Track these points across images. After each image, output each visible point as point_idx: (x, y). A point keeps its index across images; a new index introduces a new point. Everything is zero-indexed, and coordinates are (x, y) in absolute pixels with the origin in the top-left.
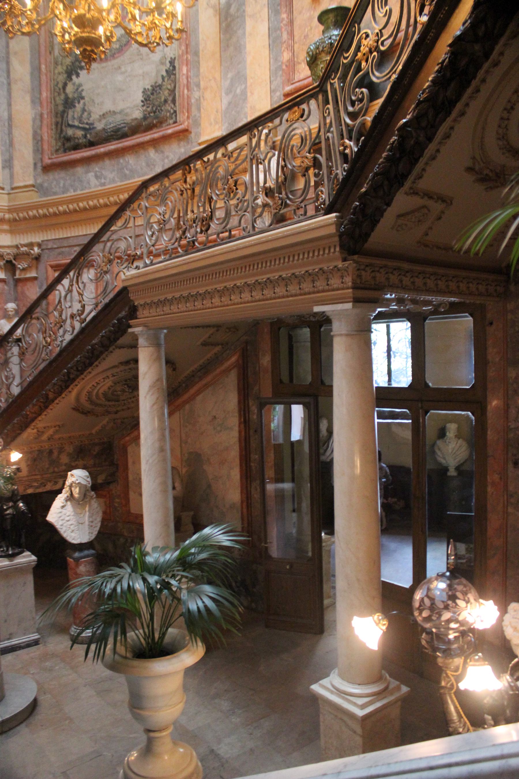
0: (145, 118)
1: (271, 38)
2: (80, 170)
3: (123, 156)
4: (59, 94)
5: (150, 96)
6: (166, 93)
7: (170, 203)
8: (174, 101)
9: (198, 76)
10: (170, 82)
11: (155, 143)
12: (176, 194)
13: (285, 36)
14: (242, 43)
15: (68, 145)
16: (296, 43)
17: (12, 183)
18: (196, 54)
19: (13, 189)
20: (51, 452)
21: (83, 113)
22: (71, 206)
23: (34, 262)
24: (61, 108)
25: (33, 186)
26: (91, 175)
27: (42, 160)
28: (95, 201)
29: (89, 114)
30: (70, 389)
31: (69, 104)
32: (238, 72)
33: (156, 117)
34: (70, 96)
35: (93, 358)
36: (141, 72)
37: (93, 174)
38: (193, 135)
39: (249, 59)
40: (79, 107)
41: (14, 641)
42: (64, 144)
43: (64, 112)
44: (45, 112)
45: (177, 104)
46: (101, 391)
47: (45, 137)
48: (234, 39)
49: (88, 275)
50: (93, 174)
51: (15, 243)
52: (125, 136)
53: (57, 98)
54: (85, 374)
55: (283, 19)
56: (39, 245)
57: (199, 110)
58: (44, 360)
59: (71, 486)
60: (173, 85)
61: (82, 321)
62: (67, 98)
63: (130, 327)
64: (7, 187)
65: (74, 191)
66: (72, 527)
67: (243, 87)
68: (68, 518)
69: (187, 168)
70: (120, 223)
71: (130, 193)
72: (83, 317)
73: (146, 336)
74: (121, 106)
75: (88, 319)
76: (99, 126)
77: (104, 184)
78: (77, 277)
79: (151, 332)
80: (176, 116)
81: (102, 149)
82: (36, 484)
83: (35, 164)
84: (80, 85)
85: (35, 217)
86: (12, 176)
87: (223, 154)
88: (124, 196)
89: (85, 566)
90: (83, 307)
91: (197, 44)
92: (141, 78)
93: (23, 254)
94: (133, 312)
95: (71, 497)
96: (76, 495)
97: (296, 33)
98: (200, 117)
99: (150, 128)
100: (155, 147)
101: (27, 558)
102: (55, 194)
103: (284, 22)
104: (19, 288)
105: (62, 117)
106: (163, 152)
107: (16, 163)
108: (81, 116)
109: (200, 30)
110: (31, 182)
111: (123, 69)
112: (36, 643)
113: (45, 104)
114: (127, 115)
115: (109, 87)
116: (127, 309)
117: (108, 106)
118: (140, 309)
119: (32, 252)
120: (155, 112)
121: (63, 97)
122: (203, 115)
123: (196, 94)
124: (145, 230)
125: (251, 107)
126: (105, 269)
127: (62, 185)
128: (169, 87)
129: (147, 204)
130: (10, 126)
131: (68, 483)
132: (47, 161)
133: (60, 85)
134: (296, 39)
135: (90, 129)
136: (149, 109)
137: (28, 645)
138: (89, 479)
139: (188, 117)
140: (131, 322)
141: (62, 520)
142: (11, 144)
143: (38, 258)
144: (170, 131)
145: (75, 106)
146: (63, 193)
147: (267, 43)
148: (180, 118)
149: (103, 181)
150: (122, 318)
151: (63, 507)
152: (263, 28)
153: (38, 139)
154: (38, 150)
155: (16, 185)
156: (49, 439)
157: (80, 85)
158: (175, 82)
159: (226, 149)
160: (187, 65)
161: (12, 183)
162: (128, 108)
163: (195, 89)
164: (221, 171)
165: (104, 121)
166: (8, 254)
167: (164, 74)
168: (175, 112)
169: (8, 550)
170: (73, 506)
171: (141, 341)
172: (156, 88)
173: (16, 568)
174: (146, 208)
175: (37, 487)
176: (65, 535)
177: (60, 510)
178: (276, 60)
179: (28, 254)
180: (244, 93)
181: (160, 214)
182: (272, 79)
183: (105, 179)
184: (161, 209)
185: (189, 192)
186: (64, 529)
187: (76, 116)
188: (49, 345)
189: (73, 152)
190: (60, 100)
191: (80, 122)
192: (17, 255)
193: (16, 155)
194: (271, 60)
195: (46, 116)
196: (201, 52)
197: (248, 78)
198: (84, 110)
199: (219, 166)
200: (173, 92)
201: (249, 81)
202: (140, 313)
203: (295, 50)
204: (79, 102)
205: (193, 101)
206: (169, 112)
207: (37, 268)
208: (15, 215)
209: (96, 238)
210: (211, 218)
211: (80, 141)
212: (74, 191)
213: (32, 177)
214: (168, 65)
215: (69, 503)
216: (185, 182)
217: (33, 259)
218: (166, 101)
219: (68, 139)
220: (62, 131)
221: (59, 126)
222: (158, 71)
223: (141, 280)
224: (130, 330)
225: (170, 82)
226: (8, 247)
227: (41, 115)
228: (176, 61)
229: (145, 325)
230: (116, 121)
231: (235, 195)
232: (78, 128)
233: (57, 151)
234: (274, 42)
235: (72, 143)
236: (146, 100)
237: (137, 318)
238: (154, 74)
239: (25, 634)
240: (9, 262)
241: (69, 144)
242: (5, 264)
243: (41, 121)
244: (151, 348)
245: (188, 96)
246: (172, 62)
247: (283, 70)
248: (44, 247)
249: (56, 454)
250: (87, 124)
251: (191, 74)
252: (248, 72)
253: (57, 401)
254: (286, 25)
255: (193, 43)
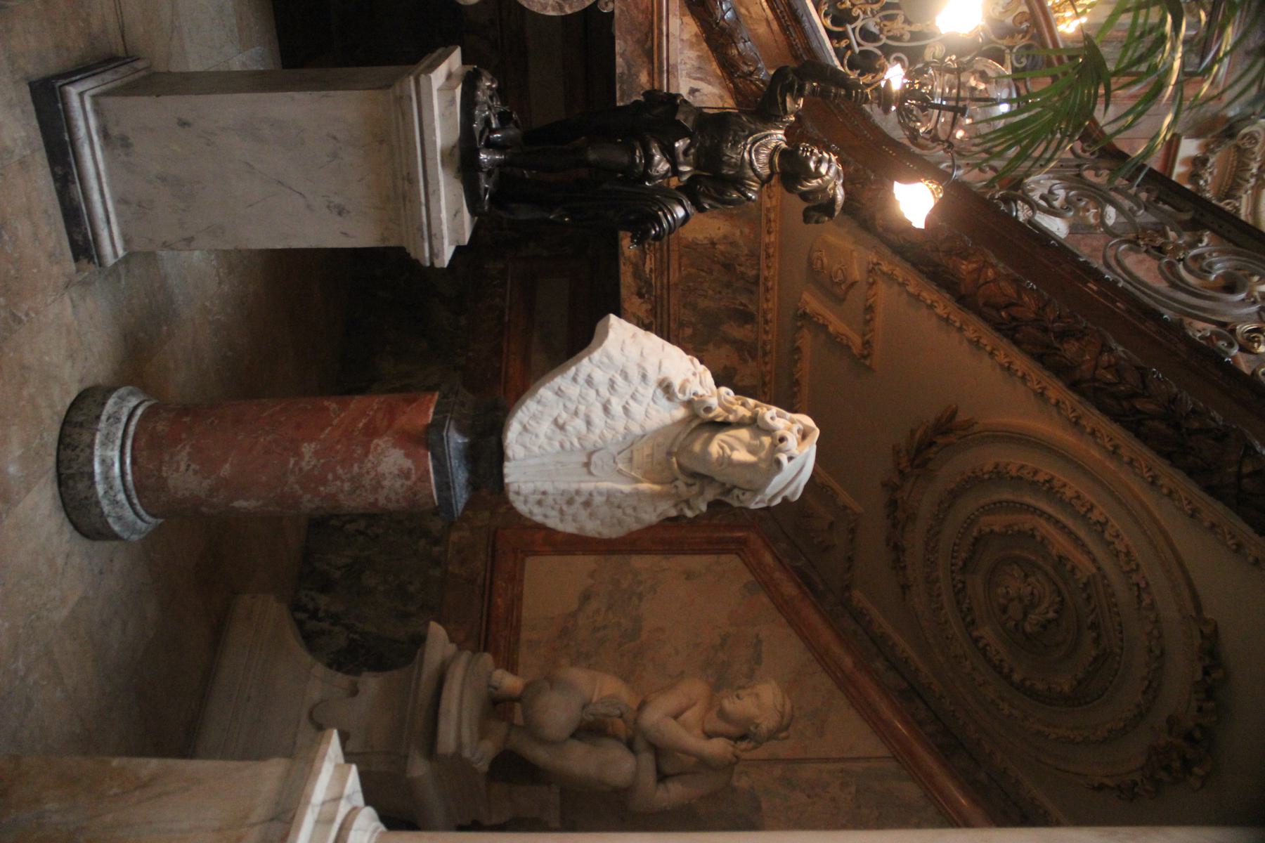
20: (745, 317)
41: (93, 158)
59: (754, 423)
66: (580, 424)
68: (616, 407)
82: (648, 266)
89: (405, 474)
95: (704, 423)
96: (717, 445)
101: (448, 223)
112: (84, 247)
131: (771, 414)
137: (74, 216)
141: (612, 384)
151: (666, 388)
169: (490, 145)
170: (662, 431)
173: (411, 181)
175: (638, 274)
176: (545, 393)
177: (653, 377)
186: (573, 391)
188: (1242, 349)
215: (680, 413)
239: (121, 201)
249: (737, 332)
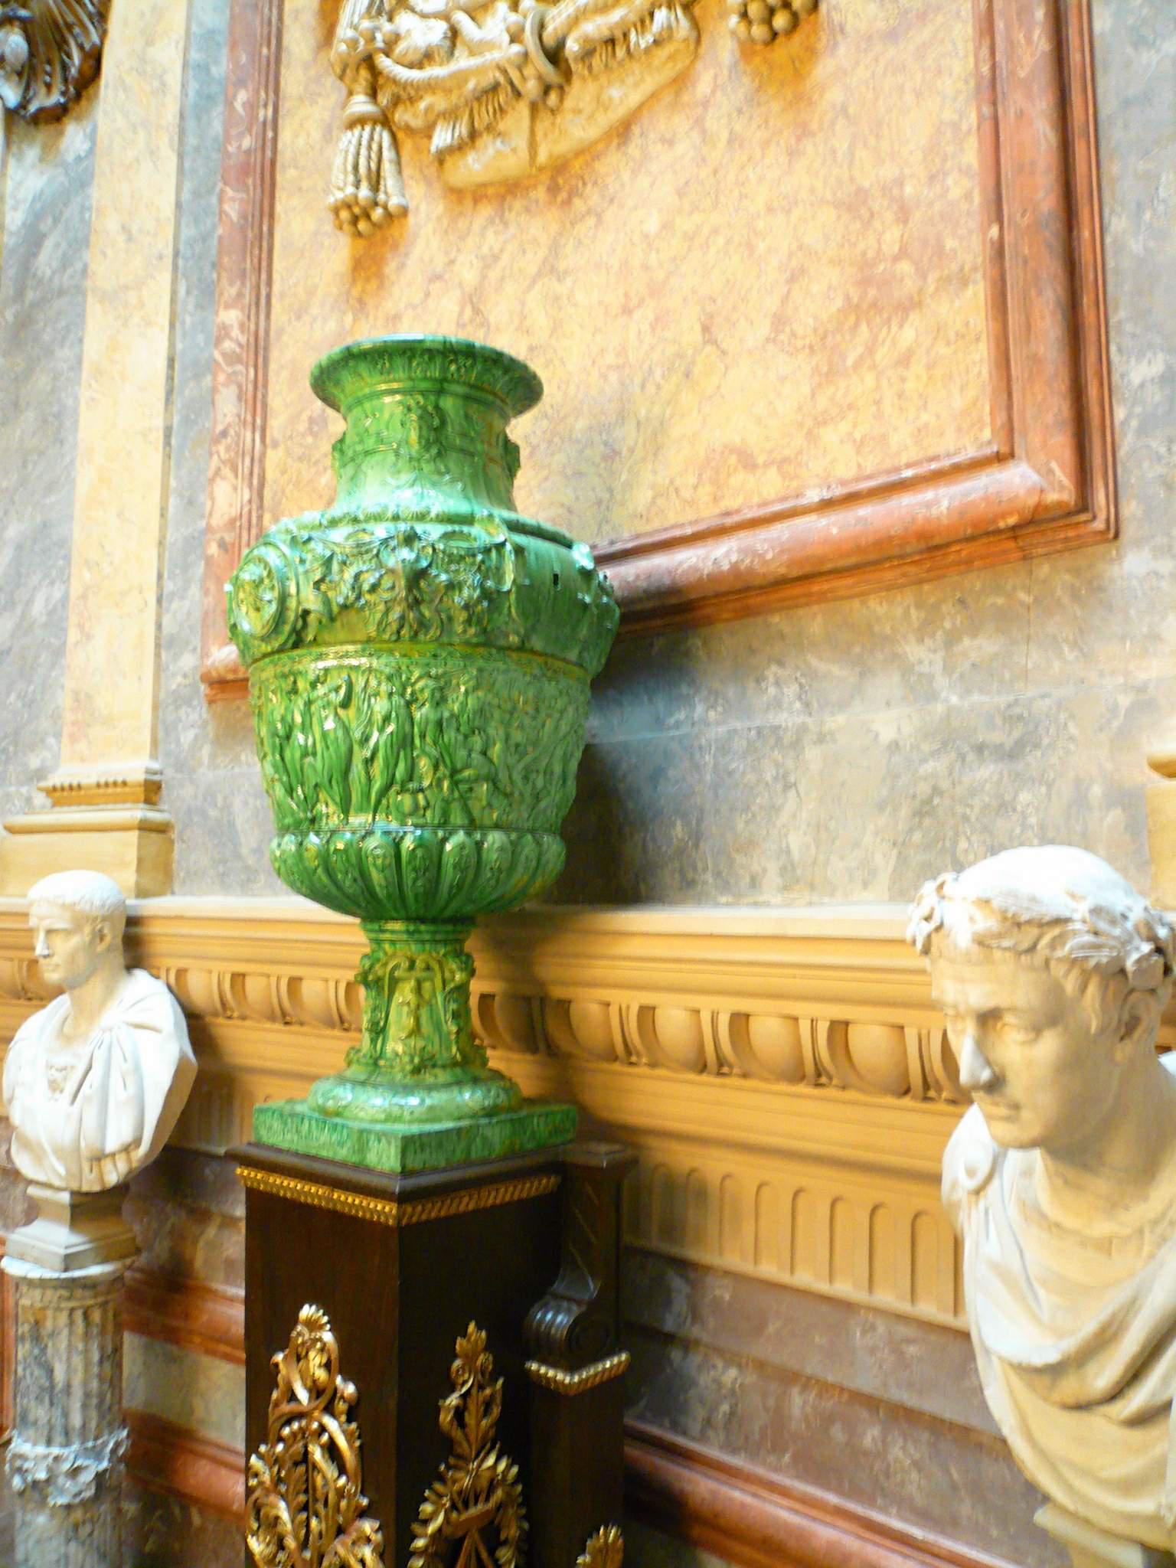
1: (178, 402)
13: (228, 407)
14: (70, 402)
16: (275, 445)
32: (45, 525)
39: (85, 478)
48: (42, 381)
55: (224, 332)
67: (57, 593)
97: (275, 402)
103: (228, 345)
125: (76, 694)
134: (276, 425)
147: (159, 423)
152: (146, 354)
178: (191, 502)
180: (56, 619)
182: (169, 586)
194: (172, 501)
197: (76, 559)
201: (80, 578)
203: (270, 475)
234: (187, 421)
247: (209, 561)
252: (77, 535)
254: (232, 358)
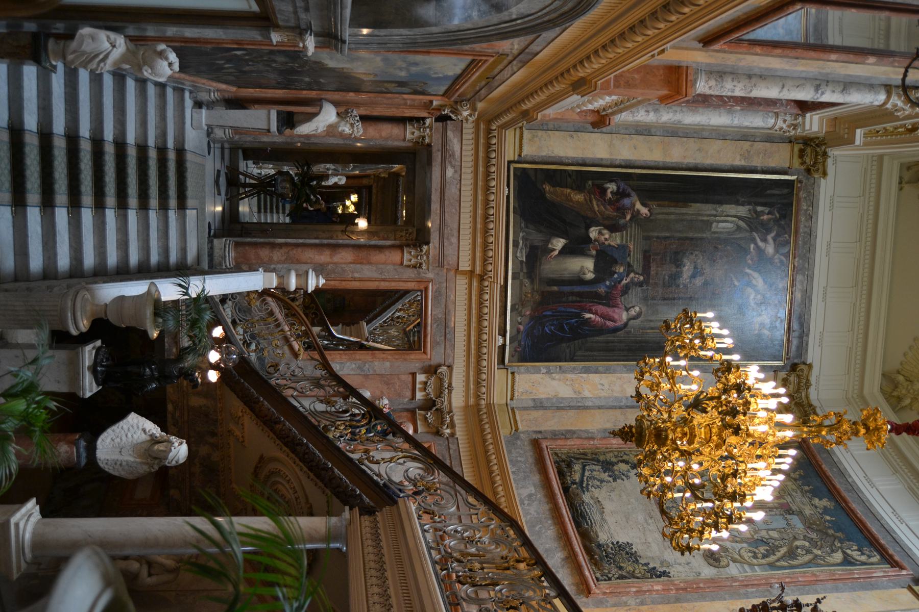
0: (599, 546)
2: (536, 478)
3: (555, 524)
4: (616, 456)
5: (624, 550)
6: (630, 568)
7: (493, 547)
8: (621, 577)
9: (654, 602)
10: (643, 572)
11: (571, 558)
12: (505, 553)
15: (563, 465)
17: (519, 409)
18: (677, 600)
19: (513, 409)
20: (214, 434)
21: (598, 480)
22: (496, 467)
23: (434, 430)
24: (602, 458)
25: (517, 430)
26: (532, 490)
27: (546, 438)
28: (502, 493)
29: (598, 487)
30: (285, 448)
31: (608, 466)
33: (601, 559)
34: (615, 467)
35: (316, 470)
36: (650, 540)
37: (533, 492)
38: (585, 599)
40: (605, 476)
42: (563, 461)
43: (598, 461)
44: (596, 442)
45: (619, 581)
46: (280, 487)
47: (569, 442)
49: (414, 469)
50: (533, 492)
51: (454, 410)
52: (578, 525)
53: (611, 454)
54: (301, 464)
56: (453, 435)
57: (614, 605)
58: (319, 422)
59: (169, 441)
60: (639, 575)
61: (361, 461)
62: (613, 464)
63: (351, 509)
64: (514, 404)
65: (513, 472)
66: (118, 440)
68: (129, 435)
69: (533, 562)
70: (471, 500)
71: (506, 510)
72: (366, 462)
73: (339, 525)
74: (610, 520)
75: (363, 467)
76: (586, 497)
77: (522, 503)
78: (410, 457)
79: (344, 530)
80: (605, 580)
81: (561, 501)
82: (177, 414)
83: (540, 432)
84: (628, 477)
85: (483, 430)
86: (525, 409)
87: (548, 594)
88: (503, 504)
89: (67, 452)
90: (378, 463)
91: (688, 601)
92: (644, 541)
93: (443, 418)
94: (368, 511)
95: (154, 440)
96: (156, 447)
98: (607, 607)
99: (589, 551)
100: (566, 558)
101: (89, 387)
102: (509, 452)
104: (405, 414)
105: (592, 460)
106: (563, 566)
107: (541, 412)
108: (595, 479)
109: (704, 603)
110: (520, 427)
111: (650, 521)
113: (604, 442)
114: (602, 526)
115: (629, 507)
116: (372, 504)
117: (608, 506)
118: (371, 519)
119: (445, 427)
120: (607, 556)
121: (614, 460)
122: (608, 610)
123: (632, 602)
124: (460, 520)
126: (419, 484)
127: (519, 459)
128: (637, 571)
129: (492, 527)
130: (578, 408)
131: (173, 438)
132: (544, 444)
133: (625, 457)
135: (582, 487)
136: (609, 550)
138: (174, 462)
139: (605, 593)
140: (357, 510)
141: (129, 430)
142: (559, 408)
143: (438, 433)
144: (587, 573)
145: (605, 472)
146: (511, 461)
148: (603, 584)
149: (526, 502)
150: (362, 499)
151: (144, 431)
153: (567, 435)
154: (555, 435)
155: (517, 412)
156: (229, 431)
157: (628, 477)
158: (643, 577)
159: (555, 597)
160: (663, 590)
161: (519, 409)
162: (609, 527)
163: (638, 601)
164: (530, 593)
165: (592, 502)
166: (442, 403)
167: (651, 566)
168: (610, 579)
169: (102, 366)
170: (143, 442)
171: (334, 520)
172: (634, 557)
173: (79, 374)
174: (488, 526)
176: (109, 431)
177: (141, 427)
179: (442, 423)
181: (480, 538)
183: (528, 505)
184: (486, 539)
185: (506, 565)
186: (118, 431)
187: (594, 473)
189: (556, 470)
190: (610, 457)
191: (589, 478)
192: (442, 412)
193: (549, 413)
195: (592, 443)
196: (680, 604)
198: (602, 481)
199: (535, 592)
200: (632, 575)
202: (366, 521)
204: (609, 476)
205: (624, 598)
206: (609, 573)
207: (428, 433)
208: (485, 410)
209: (457, 478)
210: (474, 585)
211: (568, 478)
212: (513, 472)
213: (526, 429)
214: (662, 570)
215: (148, 438)
216: (518, 561)
217: (437, 428)
218: (621, 568)
219: (569, 465)
220: (577, 459)
221: (582, 456)
222: (653, 558)
223: (404, 515)
224: (347, 508)
225: (643, 572)
226: (450, 403)
227: (593, 438)
228: (666, 578)
229: (350, 522)
230: (595, 516)
231: (499, 607)
232: (583, 475)
233: (556, 454)
235: (565, 470)
236: (619, 546)
237: (360, 515)
238: (649, 554)
240: (434, 403)
241: (564, 466)
242: (431, 399)
243: (586, 438)
244: (323, 530)
245: (629, 592)
246: (665, 574)
248: (450, 440)
250: (588, 484)
251: (654, 594)
253: (272, 435)
255: (689, 596)
